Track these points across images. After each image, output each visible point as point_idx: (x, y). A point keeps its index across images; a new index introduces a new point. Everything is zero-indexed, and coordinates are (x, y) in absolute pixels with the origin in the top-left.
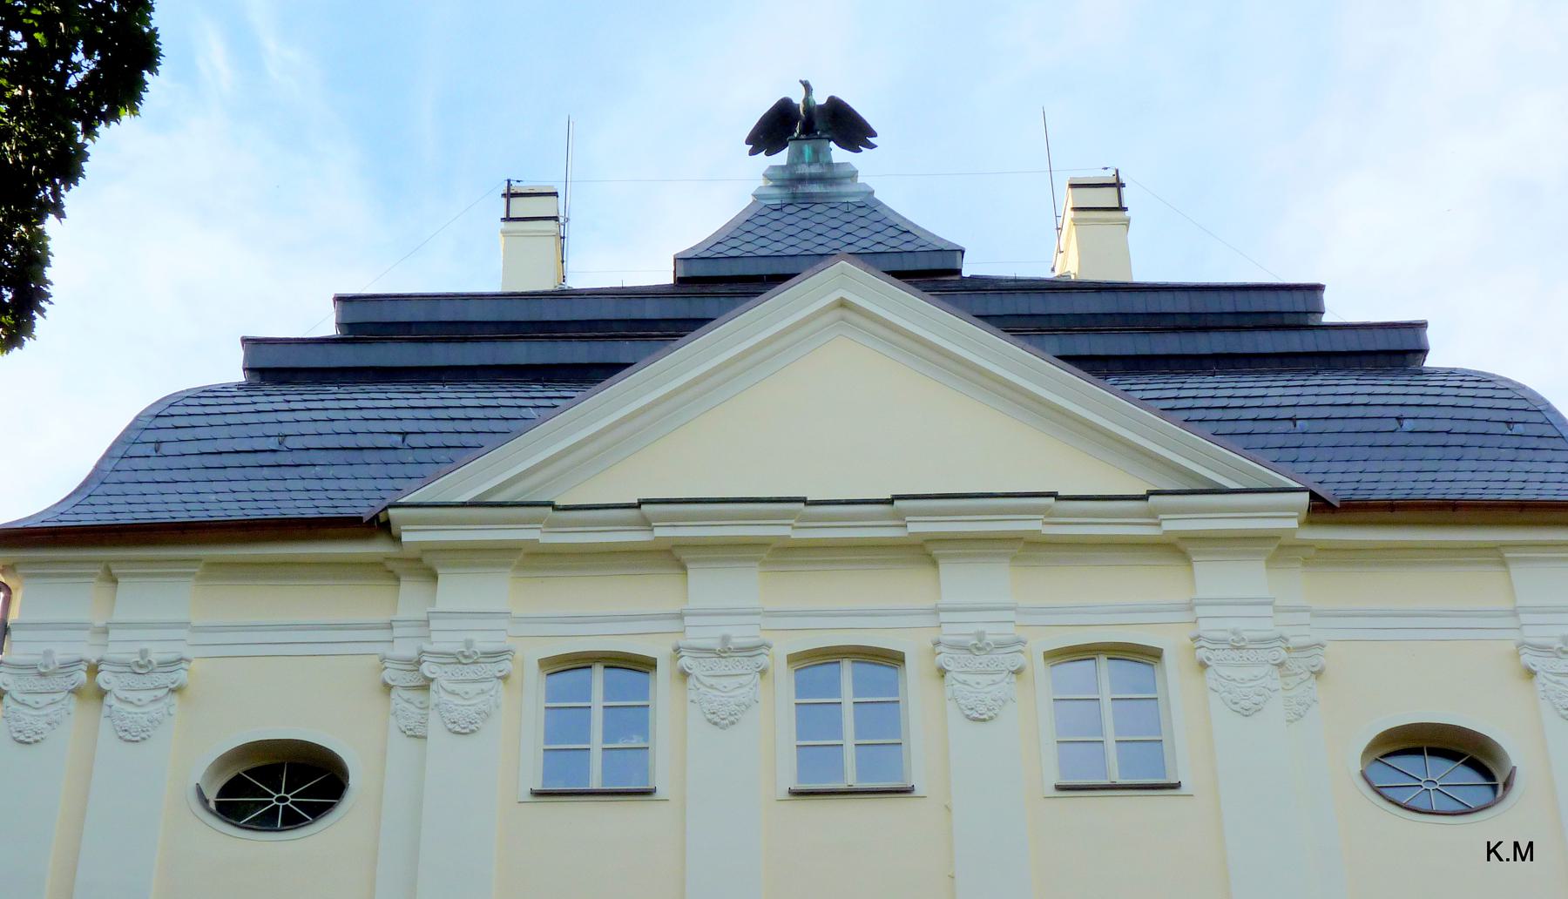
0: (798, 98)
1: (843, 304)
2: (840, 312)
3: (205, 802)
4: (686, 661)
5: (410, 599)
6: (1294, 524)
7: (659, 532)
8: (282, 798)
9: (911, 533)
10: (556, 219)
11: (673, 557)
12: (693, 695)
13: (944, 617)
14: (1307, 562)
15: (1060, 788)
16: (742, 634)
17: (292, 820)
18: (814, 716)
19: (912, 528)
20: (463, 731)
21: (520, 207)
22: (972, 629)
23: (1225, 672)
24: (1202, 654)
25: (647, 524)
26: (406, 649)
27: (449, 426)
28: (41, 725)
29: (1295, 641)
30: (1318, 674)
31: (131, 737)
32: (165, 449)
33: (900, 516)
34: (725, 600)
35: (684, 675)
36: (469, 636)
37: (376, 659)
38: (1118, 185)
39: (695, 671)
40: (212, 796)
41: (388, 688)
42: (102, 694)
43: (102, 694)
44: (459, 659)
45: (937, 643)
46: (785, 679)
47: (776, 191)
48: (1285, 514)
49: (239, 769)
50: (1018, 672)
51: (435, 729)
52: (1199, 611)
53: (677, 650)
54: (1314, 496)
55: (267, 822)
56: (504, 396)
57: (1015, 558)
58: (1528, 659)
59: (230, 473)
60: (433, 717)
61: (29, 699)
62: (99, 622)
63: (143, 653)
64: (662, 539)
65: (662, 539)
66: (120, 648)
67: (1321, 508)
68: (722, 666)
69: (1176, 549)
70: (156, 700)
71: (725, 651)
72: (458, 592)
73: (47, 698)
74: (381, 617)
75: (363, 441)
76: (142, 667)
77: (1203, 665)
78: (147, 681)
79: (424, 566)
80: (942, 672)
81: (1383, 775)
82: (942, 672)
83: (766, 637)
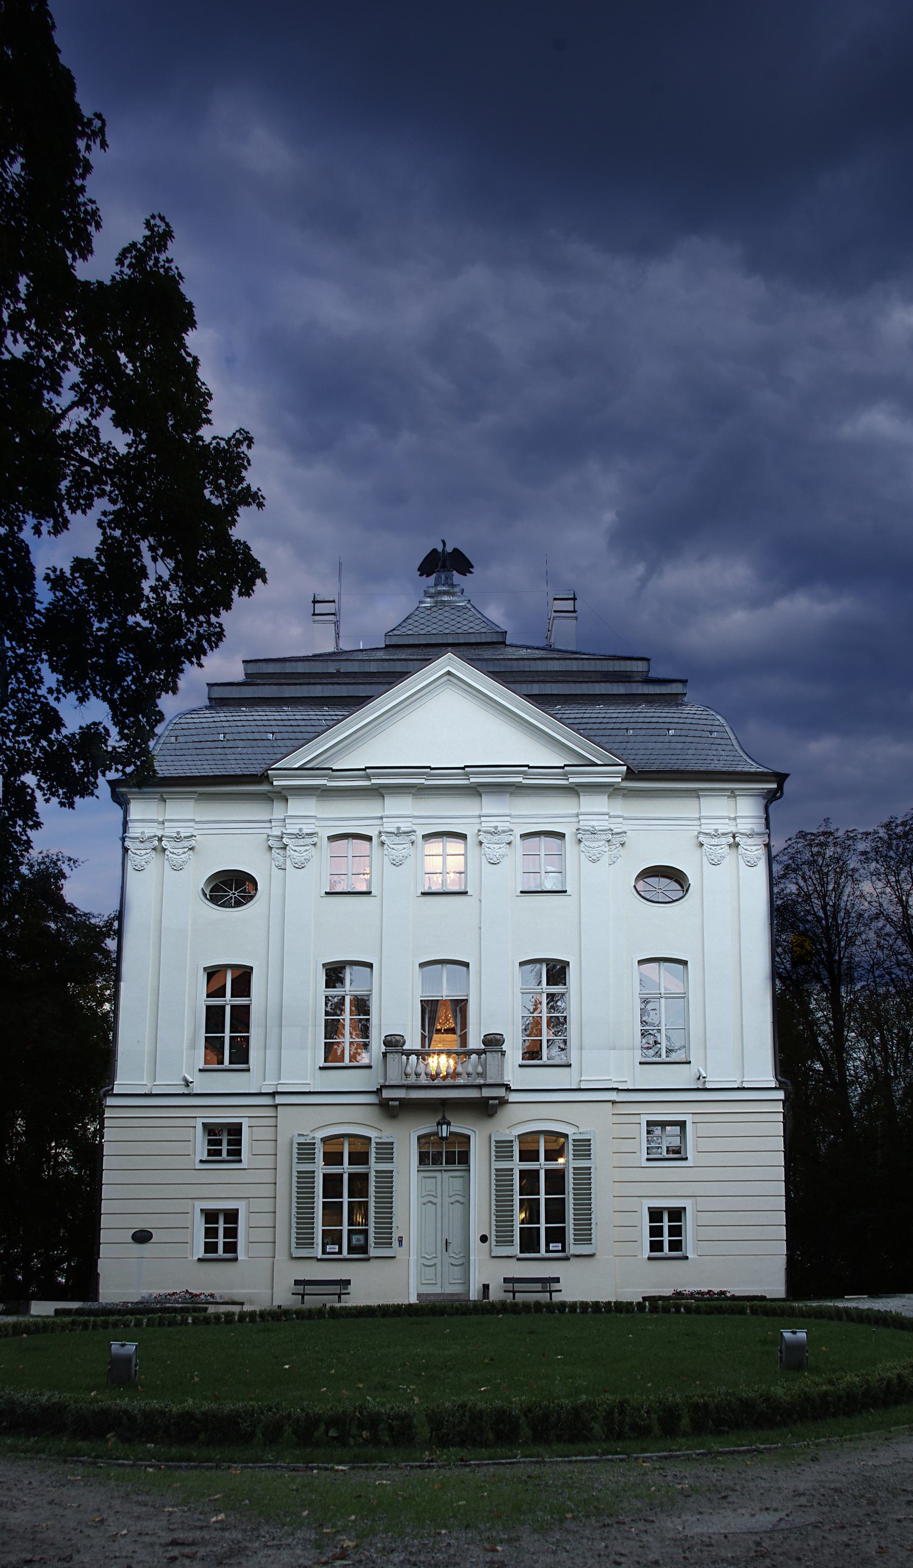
3: (205, 895)
5: (278, 810)
6: (619, 780)
7: (373, 781)
8: (233, 894)
10: (334, 614)
11: (378, 792)
12: (386, 852)
13: (483, 819)
14: (624, 796)
15: (522, 892)
16: (405, 826)
17: (238, 904)
19: (472, 780)
22: (493, 824)
23: (587, 844)
24: (579, 836)
25: (368, 777)
26: (277, 832)
27: (290, 729)
28: (143, 863)
29: (616, 831)
30: (622, 845)
31: (177, 869)
32: (180, 739)
33: (467, 774)
34: (399, 809)
35: (383, 843)
36: (301, 826)
37: (265, 836)
39: (387, 842)
40: (208, 892)
41: (270, 848)
42: (164, 850)
43: (164, 850)
44: (297, 836)
45: (479, 831)
49: (217, 882)
50: (509, 843)
51: (289, 866)
52: (581, 817)
53: (380, 833)
56: (313, 714)
57: (511, 793)
59: (205, 751)
60: (288, 860)
61: (138, 852)
62: (161, 820)
63: (178, 833)
64: (375, 786)
65: (375, 786)
66: (170, 830)
67: (630, 775)
68: (397, 840)
69: (574, 790)
70: (184, 853)
71: (398, 834)
72: (297, 807)
73: (145, 851)
74: (268, 818)
75: (257, 736)
76: (178, 839)
77: (580, 841)
78: (181, 845)
79: (283, 795)
80: (481, 843)
81: (641, 885)
82: (481, 843)
83: (414, 827)
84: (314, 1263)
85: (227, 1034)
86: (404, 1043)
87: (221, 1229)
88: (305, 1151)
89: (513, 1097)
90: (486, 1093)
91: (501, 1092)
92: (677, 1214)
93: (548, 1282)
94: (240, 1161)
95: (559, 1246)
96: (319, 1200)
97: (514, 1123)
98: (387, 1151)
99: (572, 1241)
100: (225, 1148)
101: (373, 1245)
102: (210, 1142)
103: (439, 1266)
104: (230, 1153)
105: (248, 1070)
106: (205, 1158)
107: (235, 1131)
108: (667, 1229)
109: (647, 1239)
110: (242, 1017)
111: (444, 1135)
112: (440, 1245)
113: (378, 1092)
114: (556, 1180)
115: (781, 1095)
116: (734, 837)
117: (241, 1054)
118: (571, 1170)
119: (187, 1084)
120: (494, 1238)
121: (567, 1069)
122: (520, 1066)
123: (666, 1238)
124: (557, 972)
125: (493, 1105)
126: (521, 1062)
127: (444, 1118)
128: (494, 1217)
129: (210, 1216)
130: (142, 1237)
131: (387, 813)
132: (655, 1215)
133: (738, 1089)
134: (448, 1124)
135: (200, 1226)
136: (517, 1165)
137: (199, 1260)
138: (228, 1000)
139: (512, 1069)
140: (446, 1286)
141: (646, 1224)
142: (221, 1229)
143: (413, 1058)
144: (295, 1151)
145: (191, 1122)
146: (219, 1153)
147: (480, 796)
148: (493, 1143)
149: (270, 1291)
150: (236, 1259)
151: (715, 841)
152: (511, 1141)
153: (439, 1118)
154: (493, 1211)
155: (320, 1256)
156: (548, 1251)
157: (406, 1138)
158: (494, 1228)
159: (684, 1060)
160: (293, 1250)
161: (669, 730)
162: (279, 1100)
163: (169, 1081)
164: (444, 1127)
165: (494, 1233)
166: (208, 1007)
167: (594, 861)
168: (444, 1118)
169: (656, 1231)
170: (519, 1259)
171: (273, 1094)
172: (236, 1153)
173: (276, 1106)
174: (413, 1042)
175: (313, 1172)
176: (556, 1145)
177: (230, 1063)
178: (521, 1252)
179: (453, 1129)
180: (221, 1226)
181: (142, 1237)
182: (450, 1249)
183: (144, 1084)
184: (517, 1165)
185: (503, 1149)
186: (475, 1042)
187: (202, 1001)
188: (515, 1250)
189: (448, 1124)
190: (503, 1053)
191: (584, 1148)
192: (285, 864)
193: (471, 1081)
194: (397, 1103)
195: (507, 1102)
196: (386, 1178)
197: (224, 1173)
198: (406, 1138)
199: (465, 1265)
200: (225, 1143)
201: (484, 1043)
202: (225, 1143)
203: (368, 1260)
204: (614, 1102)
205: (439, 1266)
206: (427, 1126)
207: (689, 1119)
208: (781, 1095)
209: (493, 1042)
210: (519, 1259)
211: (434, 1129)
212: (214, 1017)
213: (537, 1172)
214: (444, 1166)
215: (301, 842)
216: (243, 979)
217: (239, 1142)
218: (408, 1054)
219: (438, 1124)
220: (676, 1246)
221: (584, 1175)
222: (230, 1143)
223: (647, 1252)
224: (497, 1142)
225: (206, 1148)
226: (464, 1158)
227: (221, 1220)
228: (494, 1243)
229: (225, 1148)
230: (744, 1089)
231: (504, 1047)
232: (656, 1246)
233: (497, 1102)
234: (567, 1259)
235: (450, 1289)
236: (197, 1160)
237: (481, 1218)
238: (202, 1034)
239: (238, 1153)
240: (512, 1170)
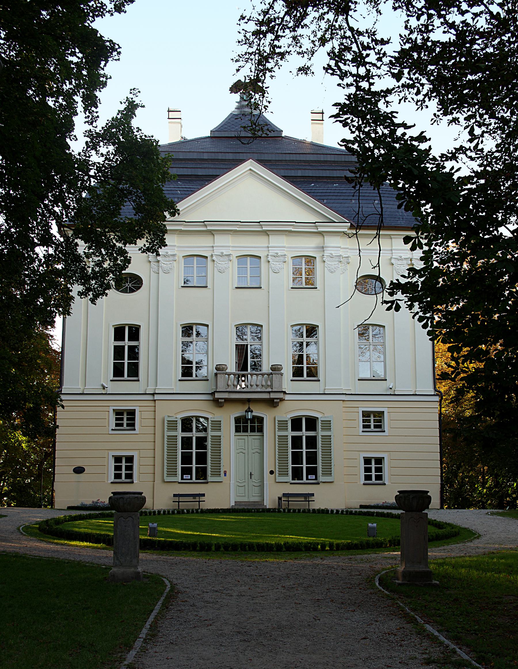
0: (243, 80)
1: (250, 170)
2: (250, 172)
4: (214, 258)
8: (129, 285)
9: (263, 230)
17: (132, 291)
18: (241, 270)
20: (166, 272)
21: (172, 115)
23: (328, 263)
35: (214, 261)
38: (323, 113)
41: (150, 262)
46: (235, 261)
47: (236, 110)
48: (345, 227)
54: (351, 224)
55: (125, 291)
58: (393, 261)
60: (160, 269)
65: (208, 229)
71: (222, 255)
82: (269, 262)
84: (177, 483)
85: (126, 361)
86: (227, 369)
87: (124, 466)
88: (172, 425)
89: (287, 397)
90: (273, 396)
91: (281, 396)
92: (379, 461)
93: (308, 496)
94: (135, 430)
95: (314, 477)
96: (180, 451)
97: (288, 411)
98: (217, 425)
99: (321, 474)
100: (125, 422)
101: (210, 475)
102: (117, 419)
103: (246, 486)
104: (128, 425)
105: (138, 380)
106: (114, 427)
107: (132, 413)
108: (374, 469)
109: (363, 474)
110: (134, 353)
111: (249, 417)
112: (247, 476)
113: (213, 394)
114: (312, 442)
115: (437, 399)
116: (411, 260)
117: (134, 371)
118: (320, 437)
119: (104, 388)
120: (277, 472)
121: (318, 382)
122: (291, 380)
123: (373, 474)
124: (312, 330)
125: (276, 402)
126: (292, 378)
127: (249, 408)
128: (277, 461)
129: (118, 459)
130: (79, 470)
131: (216, 244)
132: (367, 461)
133: (413, 395)
134: (252, 412)
135: (112, 464)
136: (290, 433)
137: (112, 483)
138: (127, 343)
139: (287, 382)
140: (250, 497)
141: (362, 466)
142: (124, 466)
143: (232, 376)
144: (166, 424)
145: (106, 409)
146: (122, 425)
147: (268, 235)
148: (277, 422)
149: (152, 500)
150: (133, 482)
151: (400, 262)
152: (287, 421)
153: (246, 408)
154: (277, 458)
155: (180, 481)
156: (307, 479)
157: (228, 417)
158: (277, 467)
159: (383, 379)
160: (165, 478)
161: (375, 200)
162: (156, 397)
163: (93, 386)
164: (249, 413)
165: (277, 469)
166: (115, 346)
167: (332, 272)
168: (249, 408)
169: (368, 470)
170: (291, 484)
171: (153, 394)
172: (132, 425)
173: (155, 400)
174: (232, 367)
175: (176, 436)
176: (312, 423)
177: (128, 376)
178: (292, 480)
179: (254, 414)
180: (124, 464)
181: (79, 470)
182: (253, 477)
183: (79, 388)
184: (290, 433)
185: (282, 425)
186: (266, 368)
187: (112, 343)
188: (289, 478)
189: (252, 412)
190: (282, 374)
191: (327, 425)
192: (158, 270)
193: (264, 390)
194: (223, 400)
195: (284, 400)
196: (217, 440)
197: (126, 435)
198: (228, 417)
199: (262, 486)
200: (125, 419)
201: (271, 369)
202: (125, 419)
203: (207, 483)
204: (343, 401)
205: (246, 486)
206: (239, 411)
207: (386, 411)
208: (437, 399)
209: (276, 369)
210: (291, 484)
211: (244, 414)
212: (118, 352)
213: (301, 437)
214: (249, 433)
215: (167, 259)
216: (135, 332)
217: (134, 419)
218: (229, 374)
219: (246, 411)
220: (379, 478)
221: (327, 439)
222: (128, 419)
223: (363, 481)
224: (279, 421)
225: (114, 422)
226: (261, 430)
227: (124, 460)
228: (277, 475)
229: (125, 422)
230: (416, 395)
231: (282, 371)
232: (368, 478)
233: (279, 400)
234: (318, 484)
235: (252, 499)
236: (110, 429)
237: (270, 461)
238: (112, 361)
239: (133, 425)
240: (287, 436)
